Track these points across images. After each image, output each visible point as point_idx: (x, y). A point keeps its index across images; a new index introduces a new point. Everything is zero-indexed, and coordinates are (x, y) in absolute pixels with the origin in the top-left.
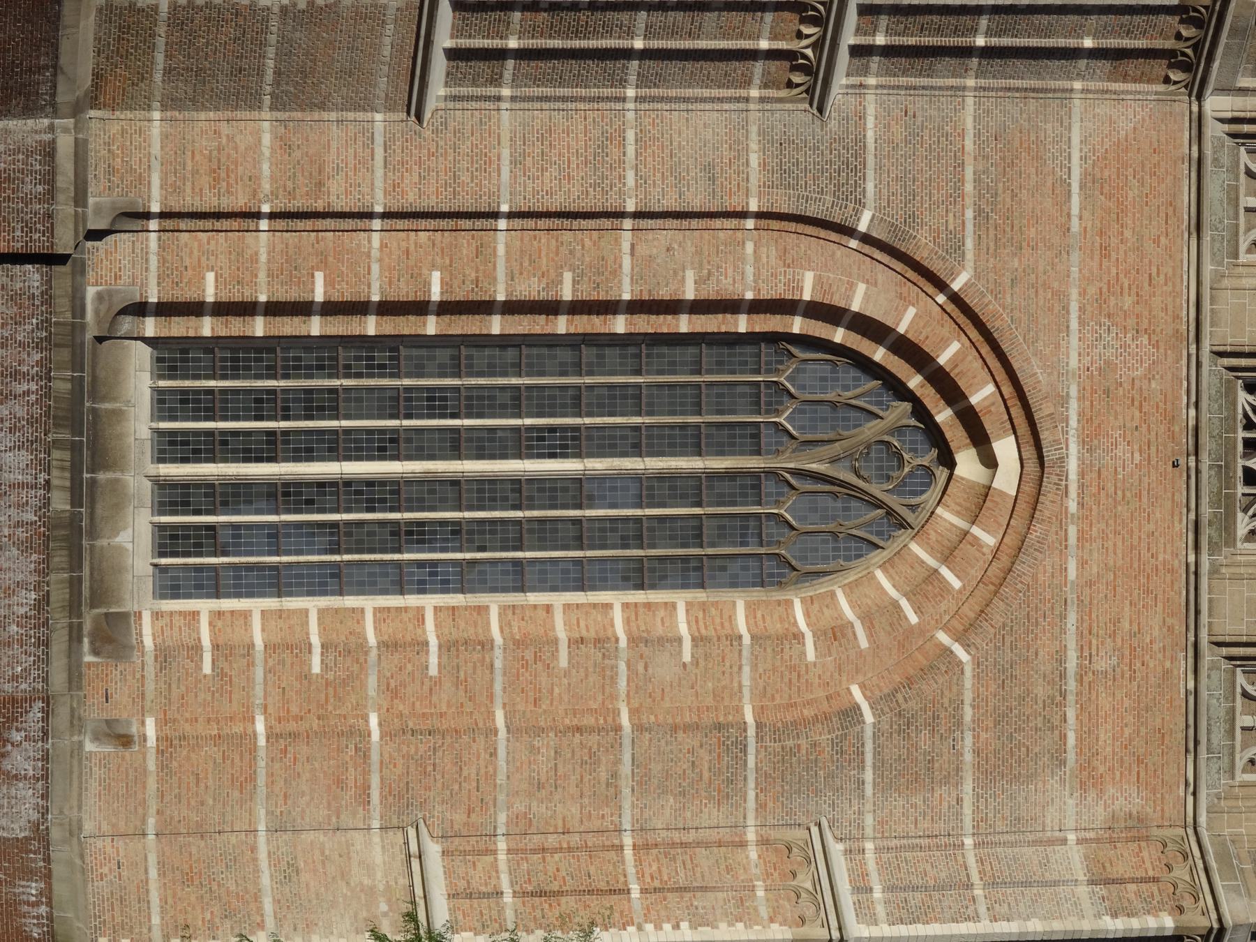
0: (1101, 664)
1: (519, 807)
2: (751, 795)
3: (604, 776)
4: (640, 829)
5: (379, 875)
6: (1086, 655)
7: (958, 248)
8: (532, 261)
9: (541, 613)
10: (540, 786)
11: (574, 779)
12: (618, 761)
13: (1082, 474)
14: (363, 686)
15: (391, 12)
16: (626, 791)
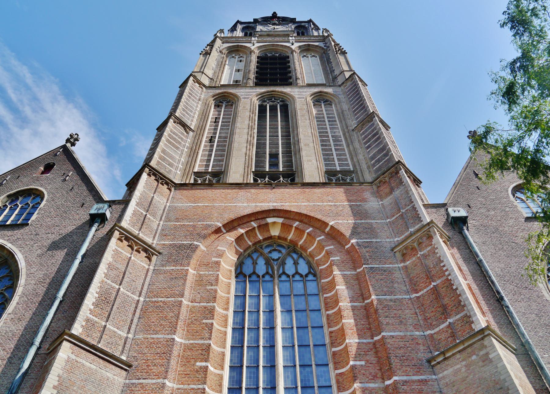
0: (331, 199)
1: (411, 328)
2: (387, 266)
3: (392, 303)
4: (407, 293)
5: (458, 366)
6: (329, 201)
7: (209, 226)
8: (197, 332)
9: (333, 335)
10: (401, 322)
11: (395, 312)
12: (385, 299)
13: (277, 203)
14: (373, 389)
15: (73, 357)
16: (396, 297)
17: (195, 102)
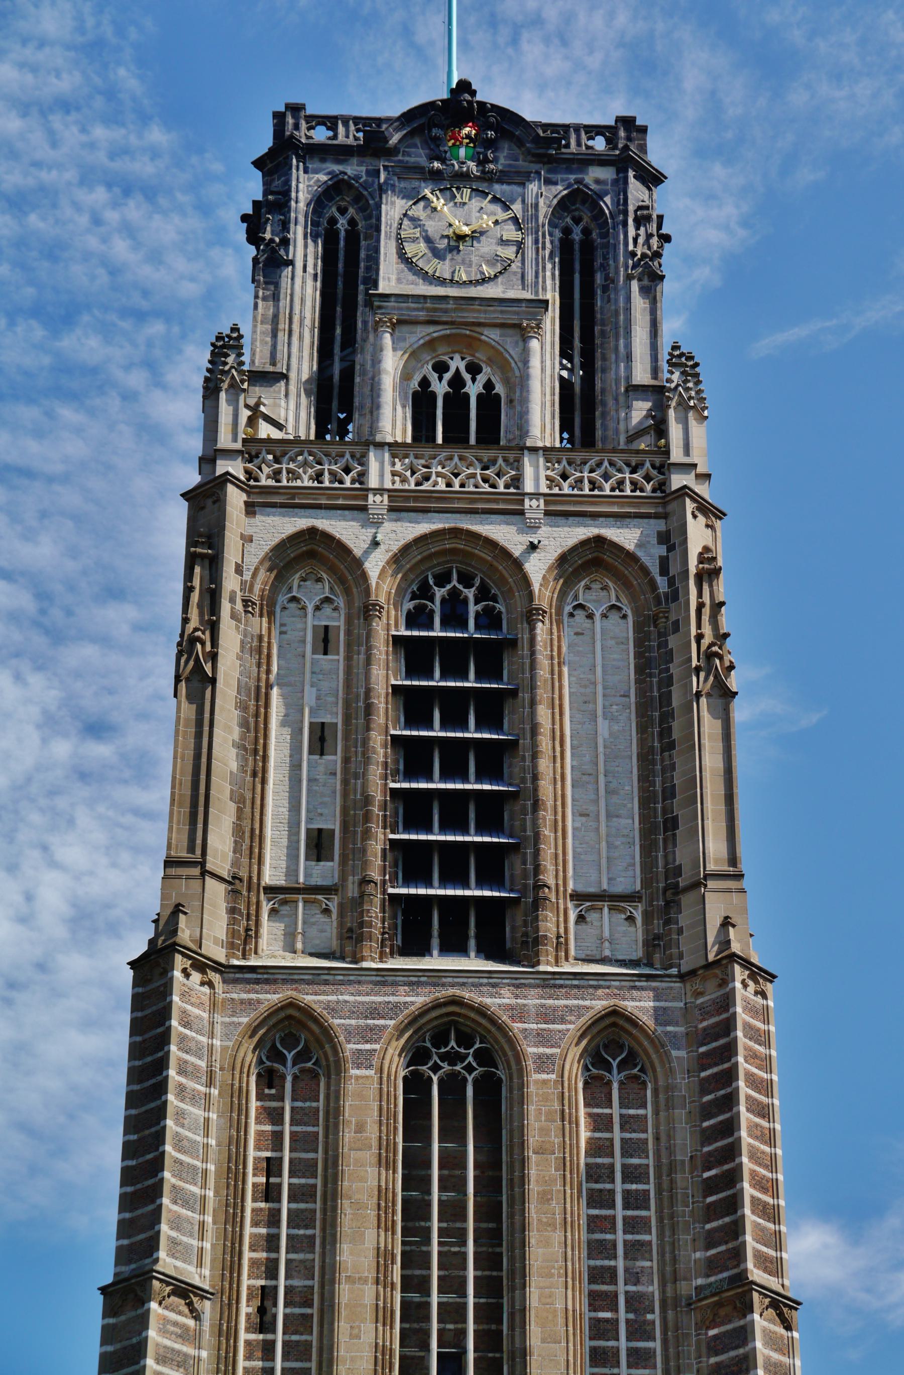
17: (194, 1099)
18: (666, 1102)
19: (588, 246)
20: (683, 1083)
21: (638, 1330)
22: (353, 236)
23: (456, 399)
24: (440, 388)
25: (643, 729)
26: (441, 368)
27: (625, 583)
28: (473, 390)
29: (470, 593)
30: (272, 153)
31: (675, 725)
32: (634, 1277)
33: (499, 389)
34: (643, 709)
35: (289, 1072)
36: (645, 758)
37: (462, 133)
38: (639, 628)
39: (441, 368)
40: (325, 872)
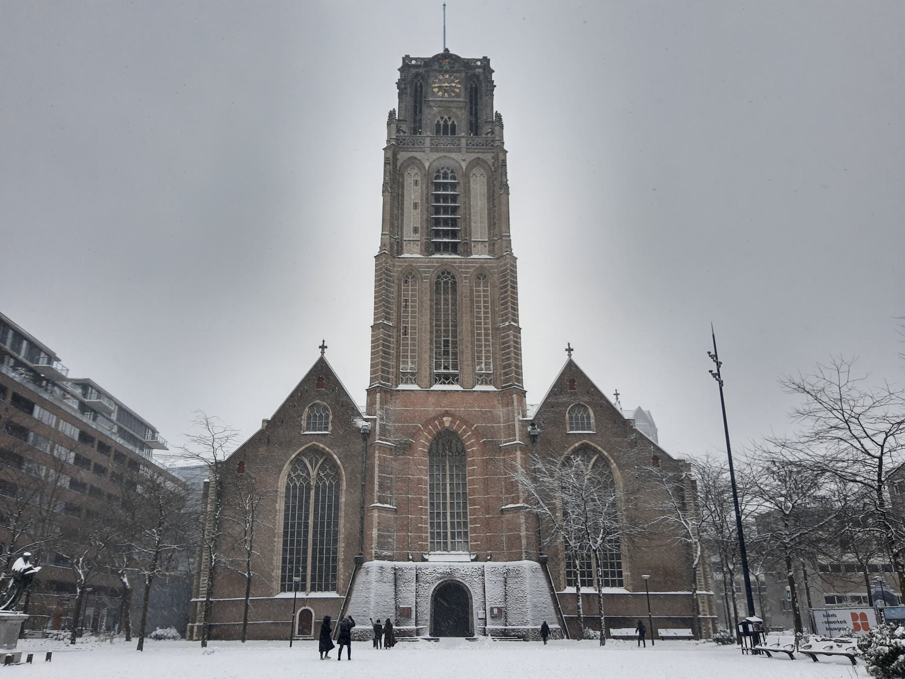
18: (493, 286)
19: (476, 88)
20: (497, 283)
21: (487, 335)
22: (421, 86)
23: (446, 125)
24: (442, 123)
25: (488, 203)
26: (442, 118)
27: (484, 168)
28: (450, 123)
29: (449, 172)
30: (402, 67)
31: (496, 202)
32: (485, 324)
33: (456, 123)
34: (488, 199)
35: (410, 280)
36: (489, 210)
37: (446, 61)
38: (488, 179)
39: (442, 118)
40: (417, 237)
